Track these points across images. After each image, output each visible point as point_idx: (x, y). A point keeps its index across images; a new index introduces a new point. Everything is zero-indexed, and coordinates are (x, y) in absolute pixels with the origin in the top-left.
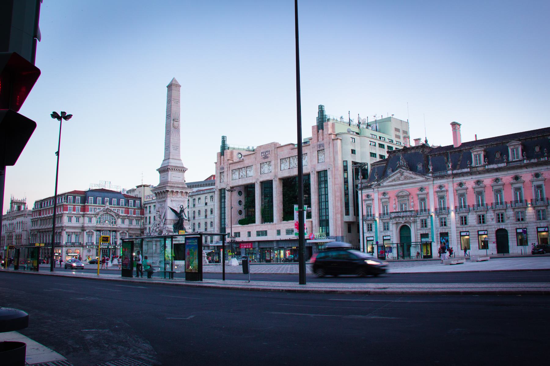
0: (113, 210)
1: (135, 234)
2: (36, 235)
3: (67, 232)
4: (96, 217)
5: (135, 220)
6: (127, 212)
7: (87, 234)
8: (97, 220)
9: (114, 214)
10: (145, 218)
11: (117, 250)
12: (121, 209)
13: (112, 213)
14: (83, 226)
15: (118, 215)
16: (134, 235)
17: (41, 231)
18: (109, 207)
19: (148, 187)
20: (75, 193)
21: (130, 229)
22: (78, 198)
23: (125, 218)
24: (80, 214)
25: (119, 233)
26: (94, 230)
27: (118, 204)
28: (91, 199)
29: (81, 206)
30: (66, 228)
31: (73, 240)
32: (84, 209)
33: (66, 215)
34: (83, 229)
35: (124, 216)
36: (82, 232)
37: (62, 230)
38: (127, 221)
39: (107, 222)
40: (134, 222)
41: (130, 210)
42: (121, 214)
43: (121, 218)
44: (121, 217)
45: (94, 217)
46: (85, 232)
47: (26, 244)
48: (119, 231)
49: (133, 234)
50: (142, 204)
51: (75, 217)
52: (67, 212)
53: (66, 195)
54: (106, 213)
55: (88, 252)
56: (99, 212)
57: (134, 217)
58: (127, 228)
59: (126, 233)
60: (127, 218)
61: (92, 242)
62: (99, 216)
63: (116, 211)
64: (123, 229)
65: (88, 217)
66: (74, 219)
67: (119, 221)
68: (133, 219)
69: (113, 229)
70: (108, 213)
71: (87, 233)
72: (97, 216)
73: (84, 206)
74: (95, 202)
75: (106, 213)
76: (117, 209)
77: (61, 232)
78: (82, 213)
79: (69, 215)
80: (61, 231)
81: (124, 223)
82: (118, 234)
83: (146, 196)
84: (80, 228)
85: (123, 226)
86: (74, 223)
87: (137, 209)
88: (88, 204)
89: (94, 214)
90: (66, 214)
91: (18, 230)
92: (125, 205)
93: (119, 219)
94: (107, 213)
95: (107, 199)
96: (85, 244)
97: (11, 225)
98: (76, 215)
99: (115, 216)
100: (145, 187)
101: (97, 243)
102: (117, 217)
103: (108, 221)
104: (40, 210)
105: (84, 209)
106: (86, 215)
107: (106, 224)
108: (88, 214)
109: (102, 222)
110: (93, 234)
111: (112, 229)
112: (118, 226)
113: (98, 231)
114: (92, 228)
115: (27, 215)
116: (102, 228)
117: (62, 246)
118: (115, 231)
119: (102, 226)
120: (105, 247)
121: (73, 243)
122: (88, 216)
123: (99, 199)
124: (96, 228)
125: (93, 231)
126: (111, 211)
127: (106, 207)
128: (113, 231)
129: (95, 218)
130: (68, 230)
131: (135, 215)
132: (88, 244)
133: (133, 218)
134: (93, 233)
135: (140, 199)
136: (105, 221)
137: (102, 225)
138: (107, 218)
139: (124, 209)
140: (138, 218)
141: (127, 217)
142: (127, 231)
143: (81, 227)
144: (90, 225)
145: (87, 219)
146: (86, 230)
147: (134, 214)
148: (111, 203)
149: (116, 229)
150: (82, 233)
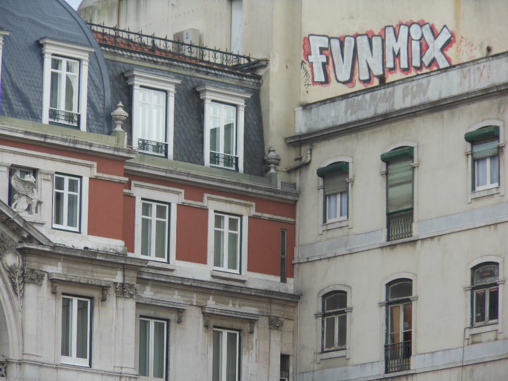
5: (194, 321)
10: (313, 305)
12: (48, 165)
23: (104, 289)
35: (87, 258)
41: (140, 192)
43: (53, 282)
44: (56, 269)
50: (275, 144)
60: (123, 291)
68: (180, 312)
81: (81, 354)
83: (316, 44)
93: (30, 289)
131: (204, 261)
133: (176, 298)
135: (249, 82)
139: (86, 172)
140: (231, 307)
141: (119, 278)
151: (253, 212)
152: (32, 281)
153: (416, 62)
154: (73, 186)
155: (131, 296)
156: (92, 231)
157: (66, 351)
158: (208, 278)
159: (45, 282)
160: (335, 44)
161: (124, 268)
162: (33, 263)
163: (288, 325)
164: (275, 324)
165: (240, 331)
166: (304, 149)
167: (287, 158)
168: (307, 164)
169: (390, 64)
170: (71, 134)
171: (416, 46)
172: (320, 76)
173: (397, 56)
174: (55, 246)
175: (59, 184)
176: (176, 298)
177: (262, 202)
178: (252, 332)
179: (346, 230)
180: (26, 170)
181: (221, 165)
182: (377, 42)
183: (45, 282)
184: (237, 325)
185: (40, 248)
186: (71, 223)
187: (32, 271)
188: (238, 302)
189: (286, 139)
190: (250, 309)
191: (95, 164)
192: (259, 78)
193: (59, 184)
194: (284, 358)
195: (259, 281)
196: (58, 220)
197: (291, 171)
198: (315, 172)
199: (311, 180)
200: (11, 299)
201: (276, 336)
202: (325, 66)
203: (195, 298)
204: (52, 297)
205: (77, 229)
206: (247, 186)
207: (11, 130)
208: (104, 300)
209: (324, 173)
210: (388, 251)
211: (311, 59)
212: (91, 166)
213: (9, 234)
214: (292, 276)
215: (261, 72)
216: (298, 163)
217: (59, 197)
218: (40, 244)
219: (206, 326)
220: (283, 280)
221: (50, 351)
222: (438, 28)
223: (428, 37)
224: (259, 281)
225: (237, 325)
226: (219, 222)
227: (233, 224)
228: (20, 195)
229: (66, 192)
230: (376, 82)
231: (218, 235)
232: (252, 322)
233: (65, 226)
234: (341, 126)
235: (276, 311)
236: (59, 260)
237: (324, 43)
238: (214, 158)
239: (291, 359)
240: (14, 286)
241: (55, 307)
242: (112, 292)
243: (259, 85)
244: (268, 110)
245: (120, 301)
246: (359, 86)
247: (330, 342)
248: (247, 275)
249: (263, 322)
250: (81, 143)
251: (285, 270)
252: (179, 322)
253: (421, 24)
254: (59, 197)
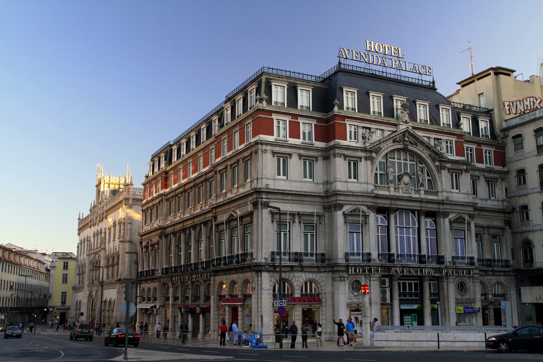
1: (488, 227)
2: (156, 246)
4: (372, 159)
5: (482, 179)
7: (345, 223)
8: (375, 172)
9: (425, 154)
10: (514, 173)
11: (445, 284)
12: (444, 137)
13: (419, 150)
14: (327, 192)
15: (437, 156)
16: (486, 232)
17: (169, 230)
18: (411, 128)
19: (509, 75)
23: (461, 170)
24: (317, 150)
25: (447, 220)
26: (368, 207)
27: (435, 118)
29: (318, 119)
30: (269, 196)
31: (297, 246)
33: (269, 148)
35: (457, 162)
36: (327, 215)
37: (255, 205)
38: (466, 180)
39: (406, 179)
40: (482, 188)
41: (465, 145)
43: (449, 169)
44: (449, 165)
45: (366, 158)
46: (339, 215)
47: (129, 278)
48: (445, 215)
49: (483, 227)
51: (300, 156)
53: (264, 78)
54: (399, 150)
55: (353, 288)
56: (380, 142)
57: (480, 170)
59: (469, 224)
60: (467, 171)
61: (366, 251)
62: (380, 158)
63: (432, 143)
64: (458, 208)
65: (345, 156)
68: (479, 177)
69: (429, 205)
70: (411, 148)
71: (345, 215)
72: (374, 155)
73: (327, 121)
74: (364, 106)
75: (400, 146)
76: (433, 136)
77: (251, 214)
78: (320, 145)
79: (277, 149)
80: (250, 208)
82: (445, 223)
83: (506, 104)
84: (318, 199)
85: (457, 196)
87: (485, 144)
88: (342, 113)
89: (364, 150)
90: (268, 143)
91: (111, 245)
93: (443, 171)
94: (405, 150)
96: (341, 260)
97: (97, 235)
98: (302, 152)
99: (429, 161)
100: (501, 76)
101: (379, 255)
102: (437, 163)
103: (410, 177)
104: (166, 173)
106: (337, 151)
107: (402, 185)
108: (348, 148)
109: (391, 178)
110: (366, 222)
111: (424, 205)
112: (441, 197)
113: (380, 210)
114: (360, 199)
115: (131, 201)
116: (393, 202)
117: (258, 269)
118: (432, 215)
119: (393, 193)
120: (410, 272)
121: (296, 254)
122: (347, 153)
124: (374, 201)
126: (418, 141)
127: (403, 127)
129: (369, 162)
132: (351, 257)
133: (477, 173)
134: (366, 216)
136: (400, 178)
137: (392, 189)
138: (405, 164)
139: (454, 139)
140: (491, 175)
142: (471, 216)
143: (323, 197)
144: (354, 186)
146: (340, 206)
147: (480, 160)
149: (436, 206)
150: (326, 219)
151: (494, 149)
152: (443, 169)
153: (532, 108)
154: (450, 143)
155: (469, 172)
156: (456, 155)
157: (453, 188)
158: (484, 167)
159: (446, 169)
160: (511, 103)
161: (466, 164)
162: (443, 164)
163: (506, 180)
164: (503, 180)
165: (494, 182)
166: (506, 132)
167: (501, 135)
168: (508, 136)
169: (526, 108)
170: (449, 129)
171: (532, 103)
172: (508, 113)
173: (527, 106)
174: (449, 159)
175: (447, 143)
176: (477, 173)
177: (496, 147)
178: (497, 182)
179: (523, 152)
180: (438, 139)
181: (484, 138)
182: (522, 103)
183: (446, 169)
184: (493, 180)
185: (445, 160)
186: (451, 153)
187: (443, 166)
188: (493, 174)
189: (500, 130)
190: (496, 176)
191: (456, 137)
192: (491, 114)
193: (447, 143)
194: (506, 189)
195: (497, 168)
196: (448, 152)
197: (502, 138)
198: (511, 138)
199: (510, 140)
200: (438, 174)
201: (503, 183)
202: (509, 109)
203: (482, 173)
204: (448, 173)
205: (452, 155)
206: (492, 143)
207: (434, 128)
208: (462, 173)
209: (514, 138)
210: (538, 156)
211: (505, 108)
212: (455, 138)
213: (436, 157)
214: (506, 167)
215: (491, 112)
216: (505, 136)
217: (447, 146)
218: (445, 158)
219: (485, 181)
220: (504, 168)
221: (449, 188)
222: (537, 98)
223: (535, 101)
224: (497, 168)
225: (493, 180)
226: (486, 152)
227: (489, 153)
228: (438, 146)
229: (449, 145)
230: (522, 113)
231: (486, 156)
232: (497, 179)
233: (449, 154)
234: (519, 124)
235: (503, 176)
236: (449, 163)
237: (508, 103)
238: (483, 136)
239: (508, 189)
240: (438, 171)
241: (449, 176)
242: (463, 171)
243: (491, 116)
244: (495, 122)
245: (466, 174)
246: (518, 115)
247: (520, 183)
248: (494, 166)
249: (500, 180)
250: (452, 131)
252: (479, 180)
253: (533, 97)
254: (447, 146)
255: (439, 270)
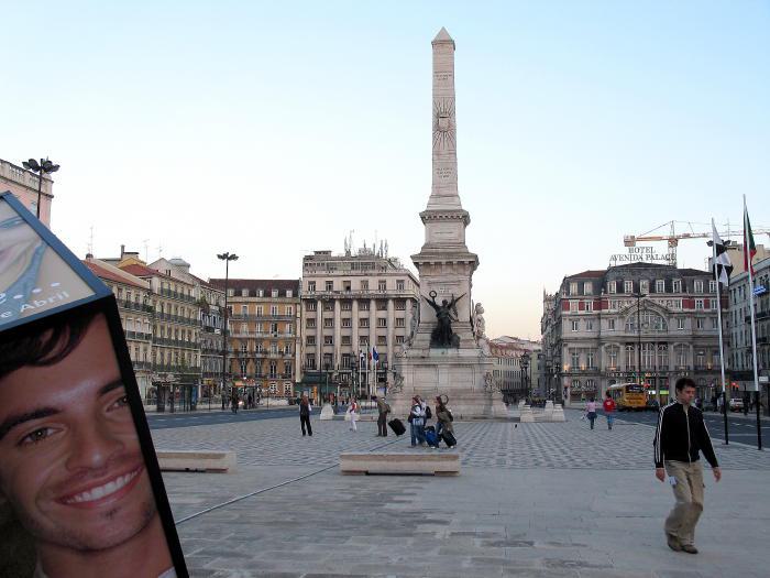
0: (657, 303)
1: (710, 347)
3: (570, 349)
5: (708, 319)
6: (689, 303)
13: (655, 309)
15: (666, 311)
20: (589, 275)
21: (695, 337)
22: (588, 288)
28: (612, 285)
32: (599, 305)
34: (599, 340)
41: (696, 300)
42: (674, 309)
48: (672, 343)
52: (569, 313)
58: (686, 336)
66: (582, 324)
67: (672, 324)
71: (606, 348)
74: (620, 289)
82: (671, 347)
86: (583, 331)
89: (617, 313)
90: (566, 315)
92: (684, 291)
95: (644, 283)
105: (599, 305)
110: (618, 352)
123: (629, 286)
125: (618, 344)
126: (654, 305)
128: (660, 343)
130: (570, 345)
142: (691, 343)
144: (613, 334)
145: (605, 324)
146: (603, 344)
148: (652, 290)
251: (727, 307)
255: (664, 373)
